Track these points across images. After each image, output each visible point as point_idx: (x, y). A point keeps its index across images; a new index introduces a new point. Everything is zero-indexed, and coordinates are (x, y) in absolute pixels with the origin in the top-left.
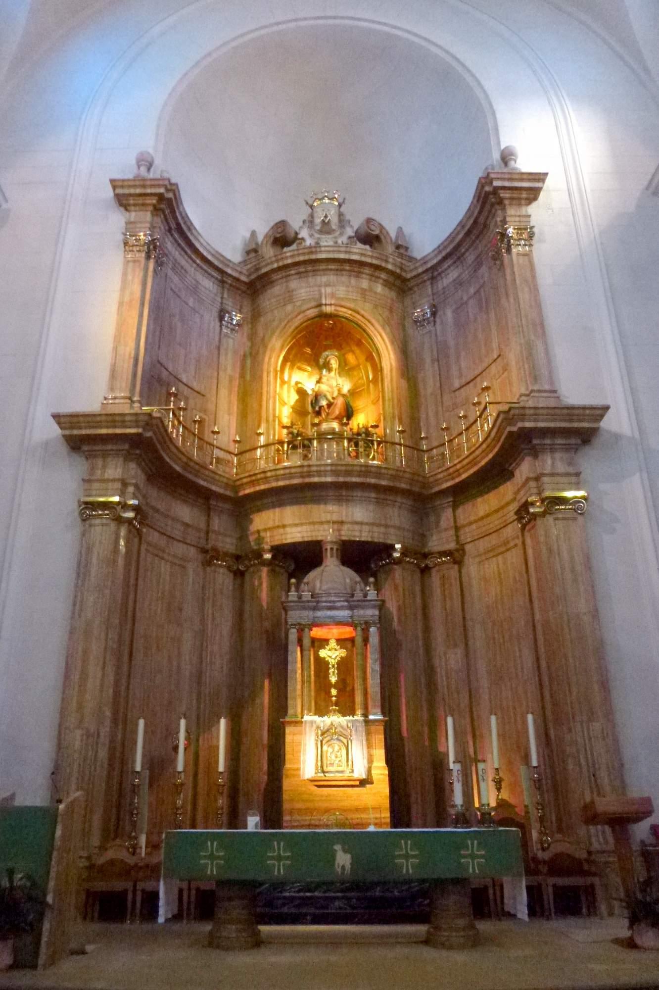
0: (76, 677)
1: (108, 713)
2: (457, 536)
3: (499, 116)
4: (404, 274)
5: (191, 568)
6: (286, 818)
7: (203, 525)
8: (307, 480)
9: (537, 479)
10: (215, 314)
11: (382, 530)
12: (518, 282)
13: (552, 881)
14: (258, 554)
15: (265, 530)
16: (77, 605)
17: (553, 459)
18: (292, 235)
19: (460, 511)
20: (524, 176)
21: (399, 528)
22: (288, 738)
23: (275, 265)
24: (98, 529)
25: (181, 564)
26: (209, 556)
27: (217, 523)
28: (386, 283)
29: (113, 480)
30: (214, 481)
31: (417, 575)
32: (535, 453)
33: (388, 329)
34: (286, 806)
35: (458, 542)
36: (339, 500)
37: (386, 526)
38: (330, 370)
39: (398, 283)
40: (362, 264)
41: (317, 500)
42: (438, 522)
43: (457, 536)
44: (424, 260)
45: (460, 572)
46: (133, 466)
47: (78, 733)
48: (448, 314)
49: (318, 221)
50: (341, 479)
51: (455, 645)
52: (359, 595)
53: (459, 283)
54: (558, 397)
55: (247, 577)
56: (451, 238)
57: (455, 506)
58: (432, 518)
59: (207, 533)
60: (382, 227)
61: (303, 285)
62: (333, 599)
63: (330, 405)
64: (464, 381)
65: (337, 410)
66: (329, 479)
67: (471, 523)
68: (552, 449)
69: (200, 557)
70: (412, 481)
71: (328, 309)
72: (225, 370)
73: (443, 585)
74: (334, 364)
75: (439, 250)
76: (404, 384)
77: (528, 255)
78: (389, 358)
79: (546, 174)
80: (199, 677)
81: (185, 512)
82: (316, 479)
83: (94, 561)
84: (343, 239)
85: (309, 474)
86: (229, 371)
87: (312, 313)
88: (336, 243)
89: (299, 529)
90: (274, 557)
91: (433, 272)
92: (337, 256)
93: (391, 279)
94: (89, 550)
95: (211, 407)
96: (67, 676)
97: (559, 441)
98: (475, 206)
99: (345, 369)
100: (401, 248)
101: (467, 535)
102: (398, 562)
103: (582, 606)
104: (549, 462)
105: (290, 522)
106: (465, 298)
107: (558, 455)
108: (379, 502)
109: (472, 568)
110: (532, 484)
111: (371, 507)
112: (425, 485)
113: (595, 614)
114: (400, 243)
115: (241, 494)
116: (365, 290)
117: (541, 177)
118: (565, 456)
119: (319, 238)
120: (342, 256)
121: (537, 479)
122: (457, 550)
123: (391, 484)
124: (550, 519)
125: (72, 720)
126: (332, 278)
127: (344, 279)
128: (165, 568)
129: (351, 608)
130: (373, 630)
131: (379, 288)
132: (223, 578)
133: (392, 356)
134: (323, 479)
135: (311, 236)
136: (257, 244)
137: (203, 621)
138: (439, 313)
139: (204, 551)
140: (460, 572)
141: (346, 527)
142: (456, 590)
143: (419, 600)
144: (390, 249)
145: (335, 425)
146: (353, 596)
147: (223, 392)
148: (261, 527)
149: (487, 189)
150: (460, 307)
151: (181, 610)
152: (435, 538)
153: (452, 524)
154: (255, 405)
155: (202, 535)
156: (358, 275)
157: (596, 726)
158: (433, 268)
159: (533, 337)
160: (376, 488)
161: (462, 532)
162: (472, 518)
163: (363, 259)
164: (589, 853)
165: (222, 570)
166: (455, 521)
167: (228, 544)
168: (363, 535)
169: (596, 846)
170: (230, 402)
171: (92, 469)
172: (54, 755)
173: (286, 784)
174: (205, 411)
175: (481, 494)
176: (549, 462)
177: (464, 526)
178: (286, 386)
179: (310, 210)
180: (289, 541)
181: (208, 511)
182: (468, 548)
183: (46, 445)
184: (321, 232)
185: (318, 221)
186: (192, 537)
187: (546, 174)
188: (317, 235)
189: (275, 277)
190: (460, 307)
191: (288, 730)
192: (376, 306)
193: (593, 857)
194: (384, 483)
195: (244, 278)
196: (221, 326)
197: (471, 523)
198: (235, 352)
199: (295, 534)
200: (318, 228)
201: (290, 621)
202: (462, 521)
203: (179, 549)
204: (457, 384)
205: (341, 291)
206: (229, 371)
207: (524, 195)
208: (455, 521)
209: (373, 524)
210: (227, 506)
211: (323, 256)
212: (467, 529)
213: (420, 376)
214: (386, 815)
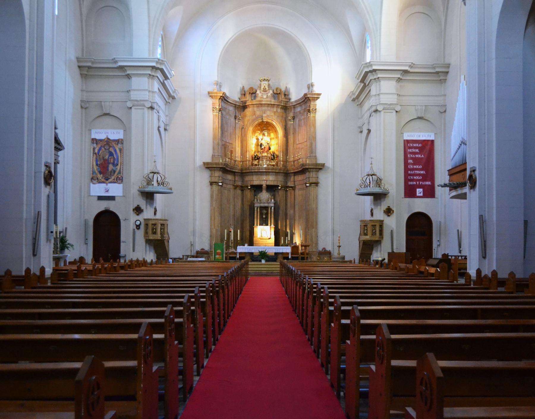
0: (213, 218)
1: (220, 226)
2: (294, 183)
3: (313, 67)
4: (286, 106)
5: (231, 190)
6: (254, 245)
7: (233, 179)
8: (259, 171)
9: (309, 178)
10: (234, 117)
11: (276, 182)
12: (311, 125)
13: (301, 256)
14: (247, 187)
15: (249, 181)
16: (211, 205)
17: (313, 174)
18: (255, 91)
19: (295, 177)
20: (315, 94)
21: (281, 181)
22: (255, 230)
23: (250, 104)
24: (214, 187)
25: (229, 190)
26: (236, 187)
27: (237, 178)
28: (281, 108)
29: (217, 177)
30: (236, 169)
31: (285, 192)
32: (309, 172)
33: (281, 123)
34: (254, 243)
35: (294, 185)
36: (266, 175)
37: (277, 181)
38: (265, 136)
39: (285, 107)
40: (274, 105)
41: (261, 175)
42: (290, 180)
43: (294, 183)
44: (292, 103)
45: (294, 192)
46: (220, 172)
47: (214, 229)
48: (297, 120)
49: (262, 87)
50: (267, 171)
51: (292, 209)
52: (270, 201)
53: (300, 112)
54: (316, 158)
55: (244, 191)
56: (299, 100)
57: (294, 176)
58: (289, 178)
59: (235, 181)
60: (280, 90)
61: (258, 110)
62: (264, 201)
63: (265, 148)
64: (299, 143)
65: (266, 149)
66: (264, 171)
67: (297, 181)
68: (313, 171)
69: (233, 187)
70: (284, 170)
71: (265, 120)
72: (237, 134)
73: (290, 195)
74: (266, 134)
75: (296, 101)
76: (285, 139)
77: (314, 117)
78: (280, 132)
79: (321, 94)
80: (234, 215)
81: (230, 177)
82: (261, 171)
83: (214, 194)
84: (269, 94)
85: (259, 170)
86: (238, 134)
87: (260, 121)
88: (267, 96)
89: (257, 182)
90: (251, 187)
91: (294, 106)
92: (267, 103)
93: (283, 107)
94: (213, 192)
95: (234, 146)
96: (211, 219)
97: (314, 170)
98: (303, 98)
99: (269, 135)
100: (286, 95)
101: (296, 183)
102: (280, 189)
103: (314, 206)
104: (312, 174)
105: (255, 180)
106: (301, 119)
107: (314, 173)
108: (276, 175)
109: (297, 191)
110: (308, 179)
111: (274, 176)
112: (287, 171)
113: (317, 208)
114: (286, 93)
115: (243, 172)
116: (275, 112)
117: (320, 94)
118: (315, 173)
119: (263, 94)
120: (269, 103)
121: (309, 178)
122: (294, 187)
123: (279, 171)
124: (310, 187)
125: (213, 227)
126: (266, 108)
127: (269, 108)
128: (226, 192)
129: (268, 203)
130: (273, 208)
131: (279, 110)
132: (239, 192)
133: (281, 133)
134: (263, 171)
135: (261, 92)
136: (245, 92)
137: (234, 202)
138: (295, 119)
139: (234, 185)
140: (294, 192)
141: (268, 181)
142: (293, 196)
143: (284, 198)
144: (283, 96)
145: (266, 154)
146: (268, 201)
147: (237, 141)
148: (248, 180)
149: (306, 97)
150: (300, 120)
151: (230, 200)
152: (289, 183)
153: (293, 180)
154: (245, 145)
155: (234, 182)
156: (273, 107)
157: (314, 230)
158: (294, 105)
159: (313, 141)
160: (275, 172)
161: (295, 182)
162: (298, 180)
163: (275, 103)
164: (309, 252)
165: (238, 190)
166: (294, 180)
167: (239, 183)
168: (272, 183)
169: (310, 251)
170: (239, 144)
171: (212, 174)
172: (210, 234)
173: (254, 239)
174: (232, 148)
175: (300, 174)
176: (312, 174)
177: (296, 181)
178: (253, 139)
179: (260, 82)
180: (255, 184)
181: (235, 175)
182: (297, 187)
183: (200, 167)
184: (263, 91)
185: (262, 87)
186: (231, 183)
187: (321, 94)
188: (262, 92)
189: (250, 106)
190: (300, 120)
191: (255, 228)
192: (278, 116)
193: (310, 253)
194: (277, 171)
195: (241, 105)
196: (235, 121)
197: (297, 181)
198: (239, 128)
199: (256, 183)
200: (262, 90)
201: (255, 206)
202: (296, 180)
203: (229, 186)
204: (297, 143)
205: (268, 113)
206: (238, 134)
207: (316, 99)
208: (294, 180)
209: (274, 181)
210: (239, 174)
211: (264, 103)
212: (297, 182)
213: (289, 137)
214: (274, 245)
